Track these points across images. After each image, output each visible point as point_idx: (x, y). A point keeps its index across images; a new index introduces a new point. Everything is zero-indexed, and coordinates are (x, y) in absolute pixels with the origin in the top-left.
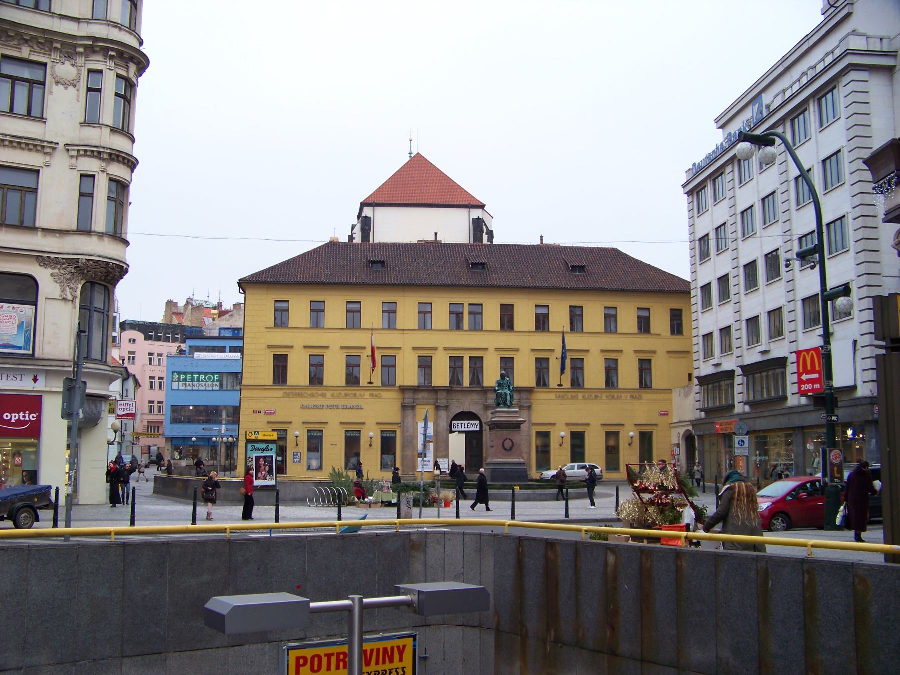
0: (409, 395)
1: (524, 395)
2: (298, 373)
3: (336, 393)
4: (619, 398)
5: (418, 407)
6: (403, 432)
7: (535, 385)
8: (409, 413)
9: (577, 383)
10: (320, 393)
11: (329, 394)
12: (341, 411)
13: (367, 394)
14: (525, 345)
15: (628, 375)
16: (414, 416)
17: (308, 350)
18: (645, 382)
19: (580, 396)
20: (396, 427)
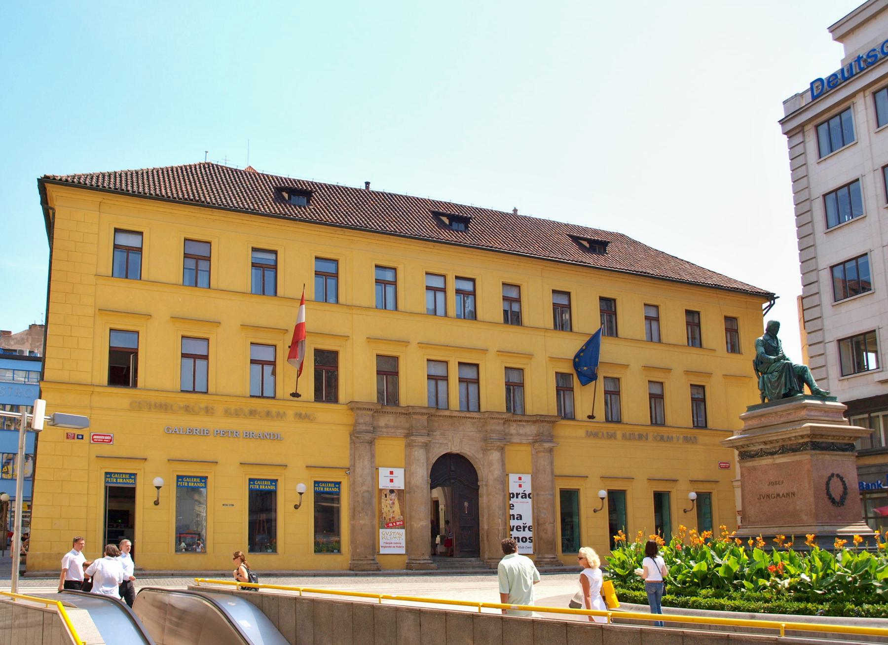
2: (158, 366)
4: (670, 439)
6: (353, 485)
7: (555, 412)
9: (613, 417)
15: (678, 408)
16: (373, 456)
18: (700, 421)
19: (619, 435)
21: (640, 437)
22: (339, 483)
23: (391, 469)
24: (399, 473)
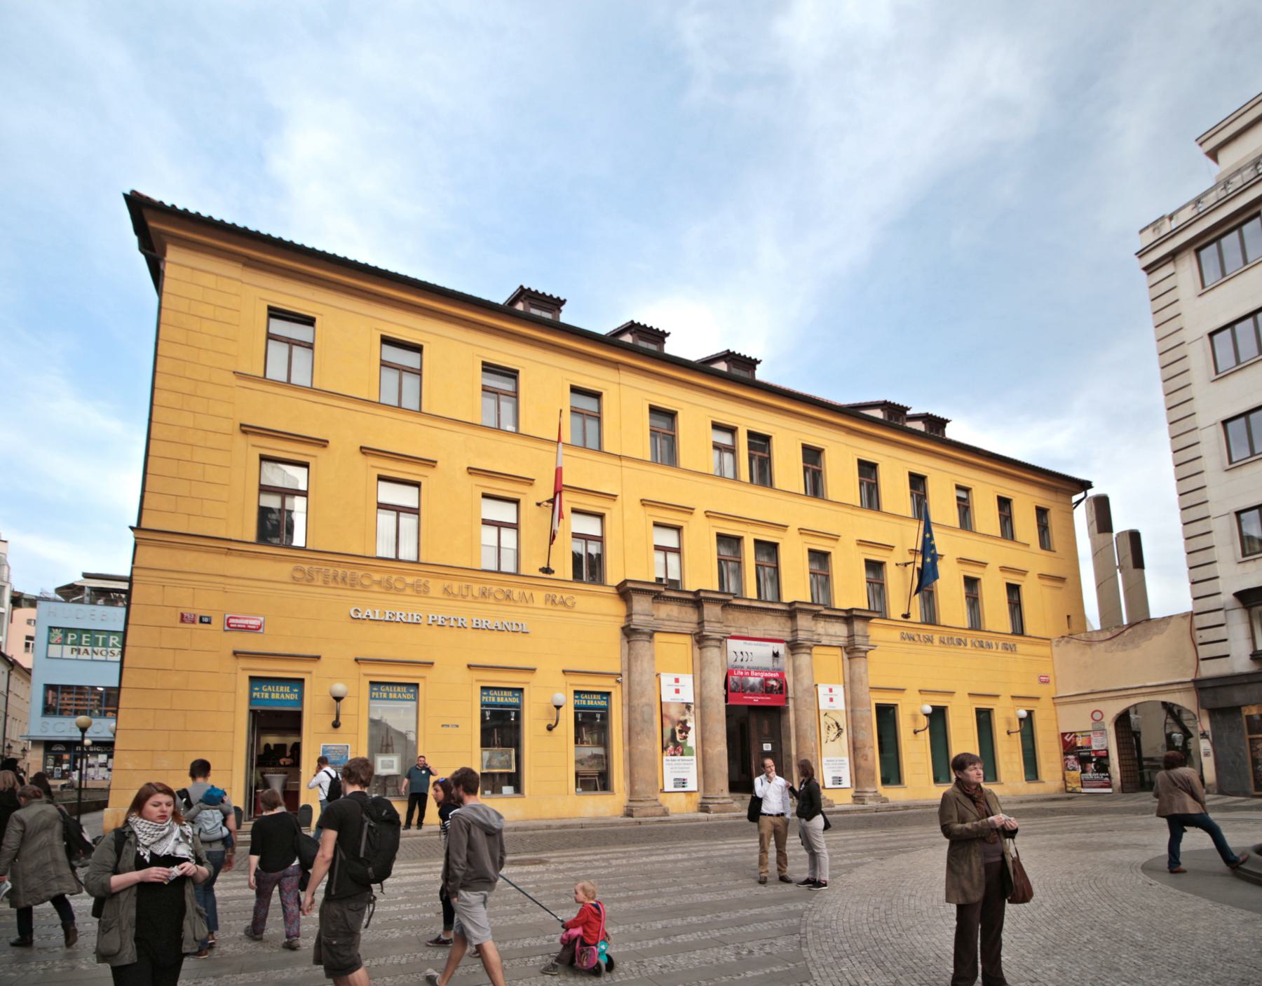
0: (641, 604)
1: (858, 626)
3: (455, 586)
5: (656, 635)
8: (641, 646)
10: (409, 580)
11: (436, 586)
12: (470, 634)
13: (539, 596)
14: (851, 531)
17: (373, 461)
20: (611, 682)
21: (959, 642)
22: (609, 694)
23: (677, 676)
24: (687, 681)
